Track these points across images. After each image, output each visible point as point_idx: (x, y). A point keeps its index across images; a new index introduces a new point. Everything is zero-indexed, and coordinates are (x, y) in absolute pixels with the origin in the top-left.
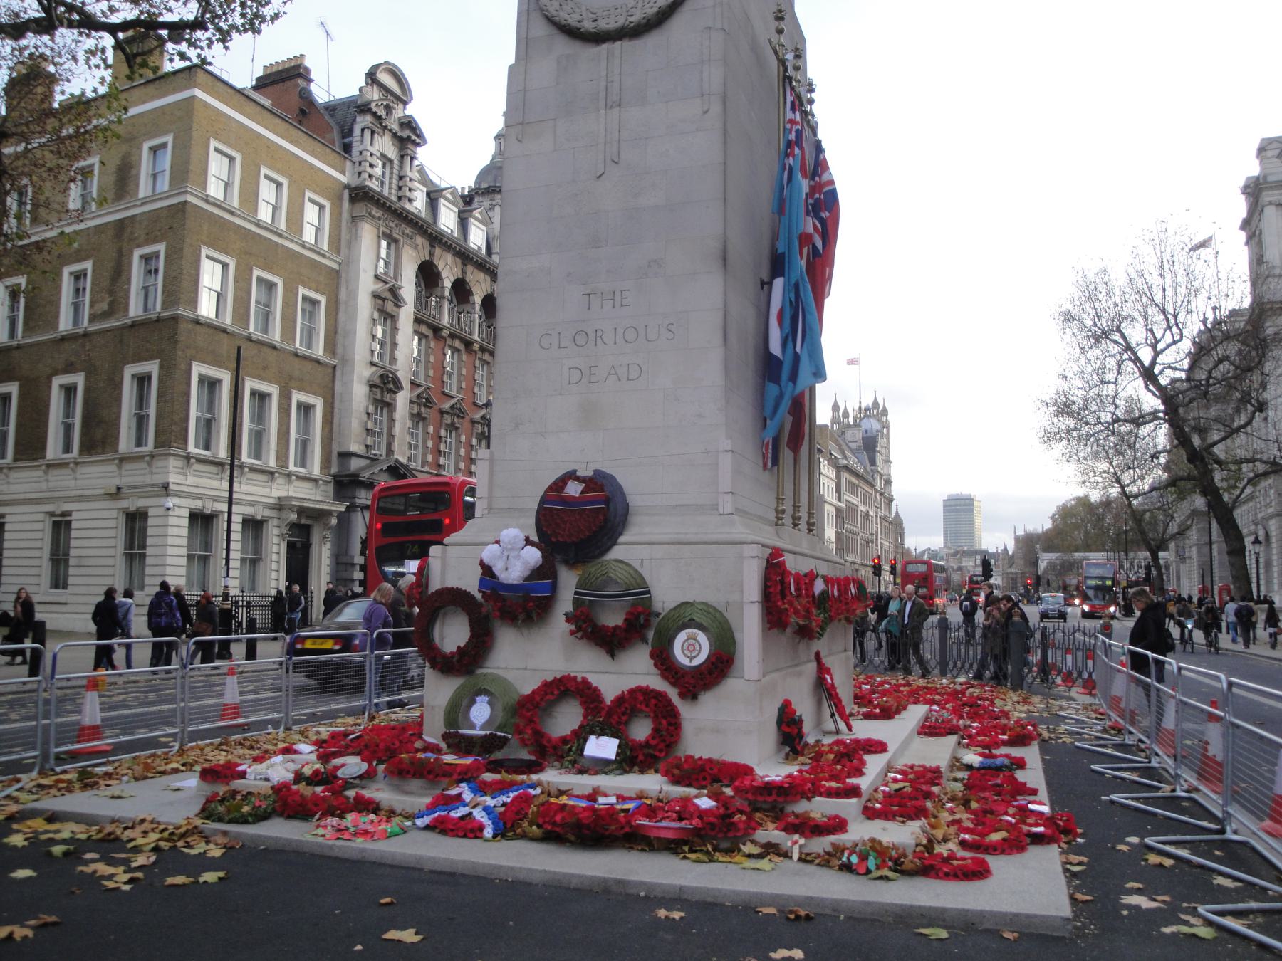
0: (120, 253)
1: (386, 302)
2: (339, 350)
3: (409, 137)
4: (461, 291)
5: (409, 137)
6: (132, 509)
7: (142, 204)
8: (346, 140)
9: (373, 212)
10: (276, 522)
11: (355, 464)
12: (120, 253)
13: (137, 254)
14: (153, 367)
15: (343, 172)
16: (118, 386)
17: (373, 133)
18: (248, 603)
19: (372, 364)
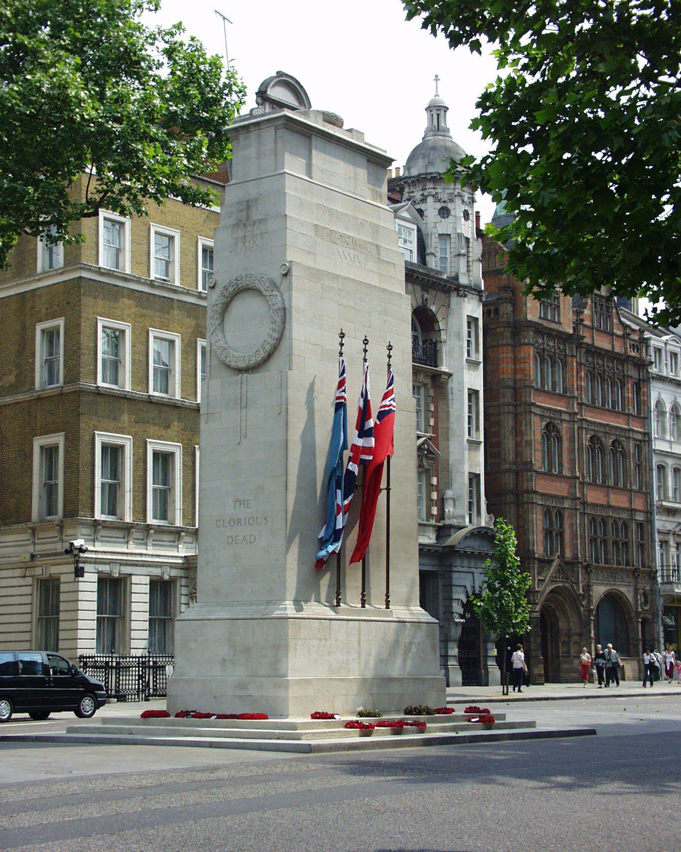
0: (24, 328)
6: (46, 576)
7: (40, 280)
10: (183, 581)
12: (24, 328)
13: (39, 328)
14: (58, 439)
16: (28, 456)
18: (155, 663)
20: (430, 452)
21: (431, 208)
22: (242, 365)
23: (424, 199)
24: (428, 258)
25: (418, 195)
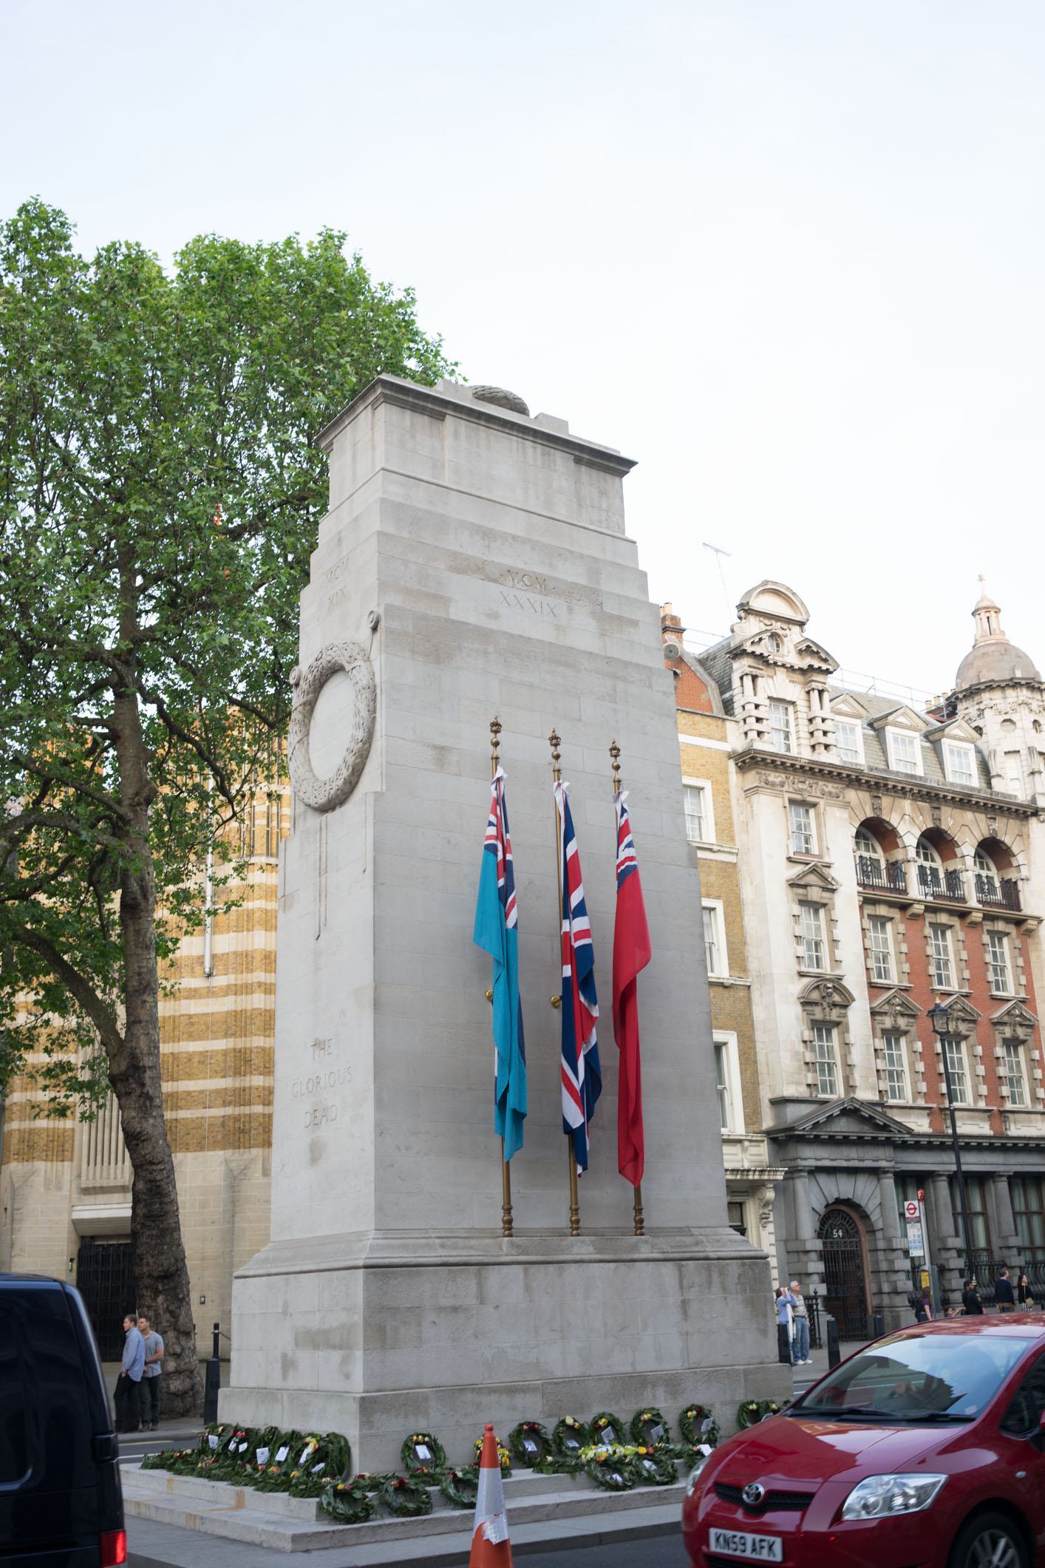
1: (811, 888)
2: (753, 965)
3: (811, 666)
4: (936, 840)
5: (811, 666)
8: (727, 695)
9: (771, 779)
11: (793, 1113)
15: (724, 739)
17: (754, 678)
19: (801, 975)
20: (1021, 1015)
21: (991, 722)
22: (322, 800)
23: (981, 713)
24: (994, 781)
25: (973, 711)
